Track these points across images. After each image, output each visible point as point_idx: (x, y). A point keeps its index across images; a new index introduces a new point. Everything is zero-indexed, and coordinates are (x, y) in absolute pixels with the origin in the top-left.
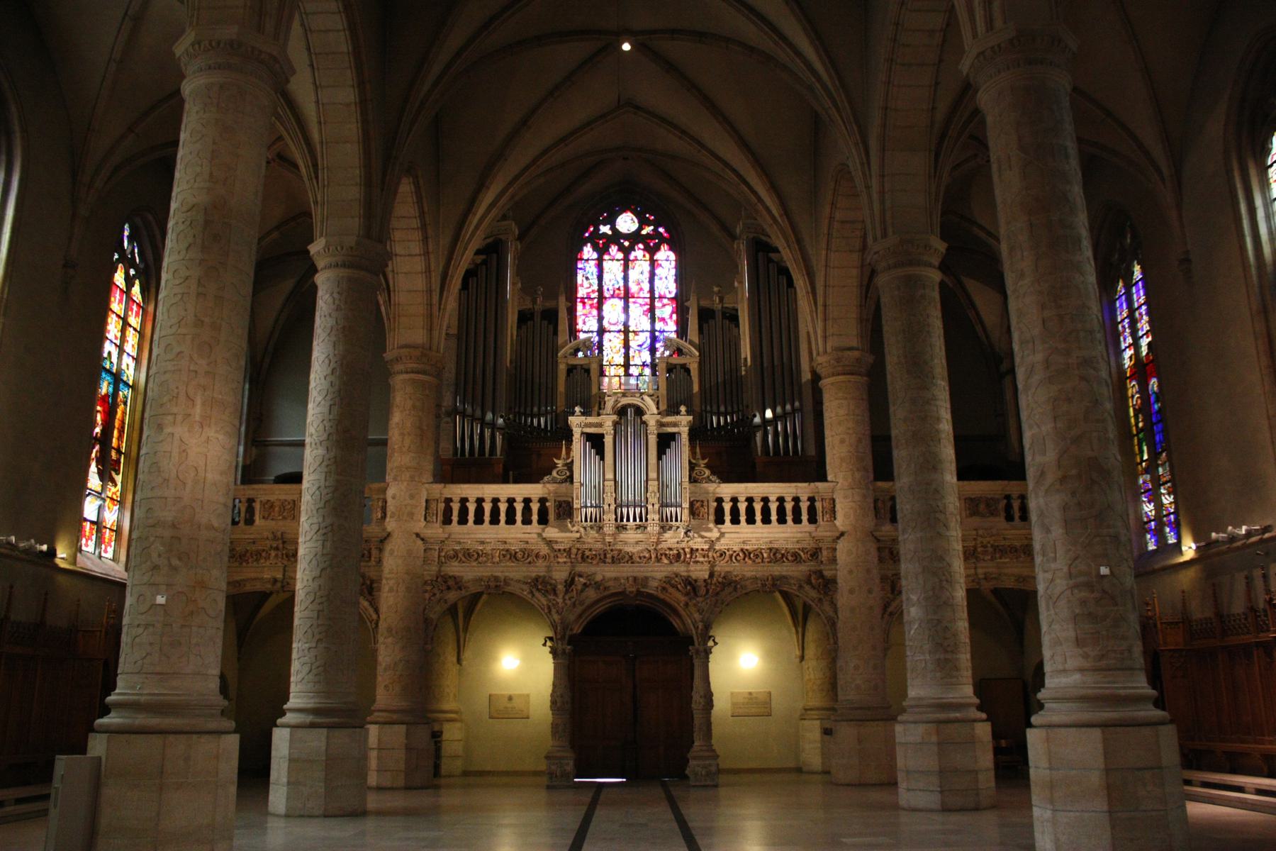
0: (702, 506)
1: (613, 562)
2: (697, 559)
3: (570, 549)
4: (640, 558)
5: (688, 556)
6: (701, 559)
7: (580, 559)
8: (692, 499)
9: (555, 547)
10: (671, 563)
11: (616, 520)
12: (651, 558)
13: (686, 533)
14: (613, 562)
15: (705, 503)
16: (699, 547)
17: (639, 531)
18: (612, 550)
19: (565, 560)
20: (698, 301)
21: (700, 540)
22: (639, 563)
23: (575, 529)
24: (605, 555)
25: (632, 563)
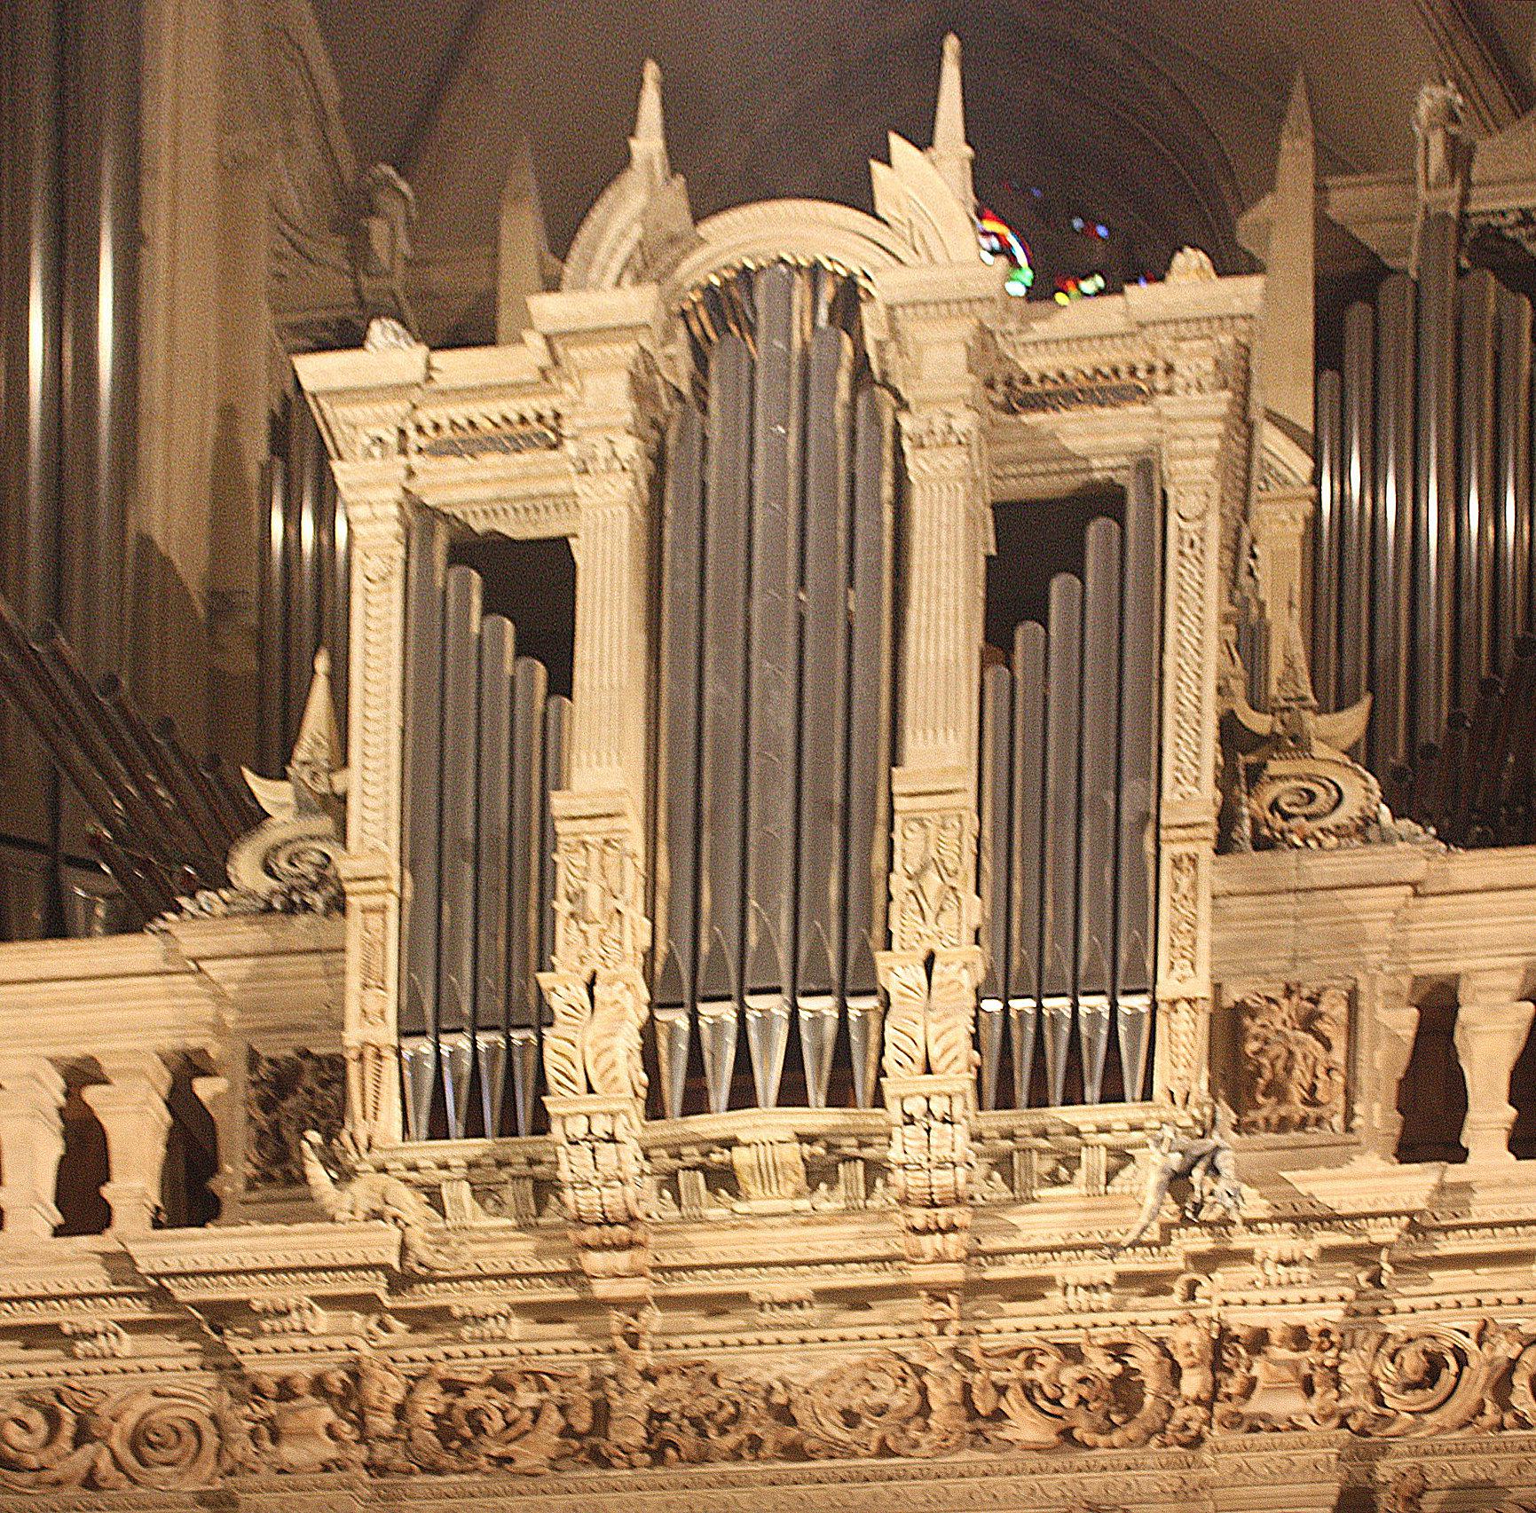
0: (1308, 1022)
1: (657, 1450)
2: (1257, 1404)
3: (356, 1374)
4: (850, 1418)
5: (1193, 1382)
6: (1291, 1404)
7: (427, 1439)
8: (1233, 995)
9: (251, 1365)
10: (1067, 1434)
11: (654, 1108)
12: (925, 1410)
13: (1178, 1182)
14: (657, 1450)
15: (1333, 1007)
16: (1276, 1320)
17: (827, 1201)
18: (649, 1376)
19: (330, 1450)
20: (1320, 189)
21: (1280, 1241)
22: (833, 1450)
23: (361, 1192)
24: (602, 1412)
25: (794, 1451)
